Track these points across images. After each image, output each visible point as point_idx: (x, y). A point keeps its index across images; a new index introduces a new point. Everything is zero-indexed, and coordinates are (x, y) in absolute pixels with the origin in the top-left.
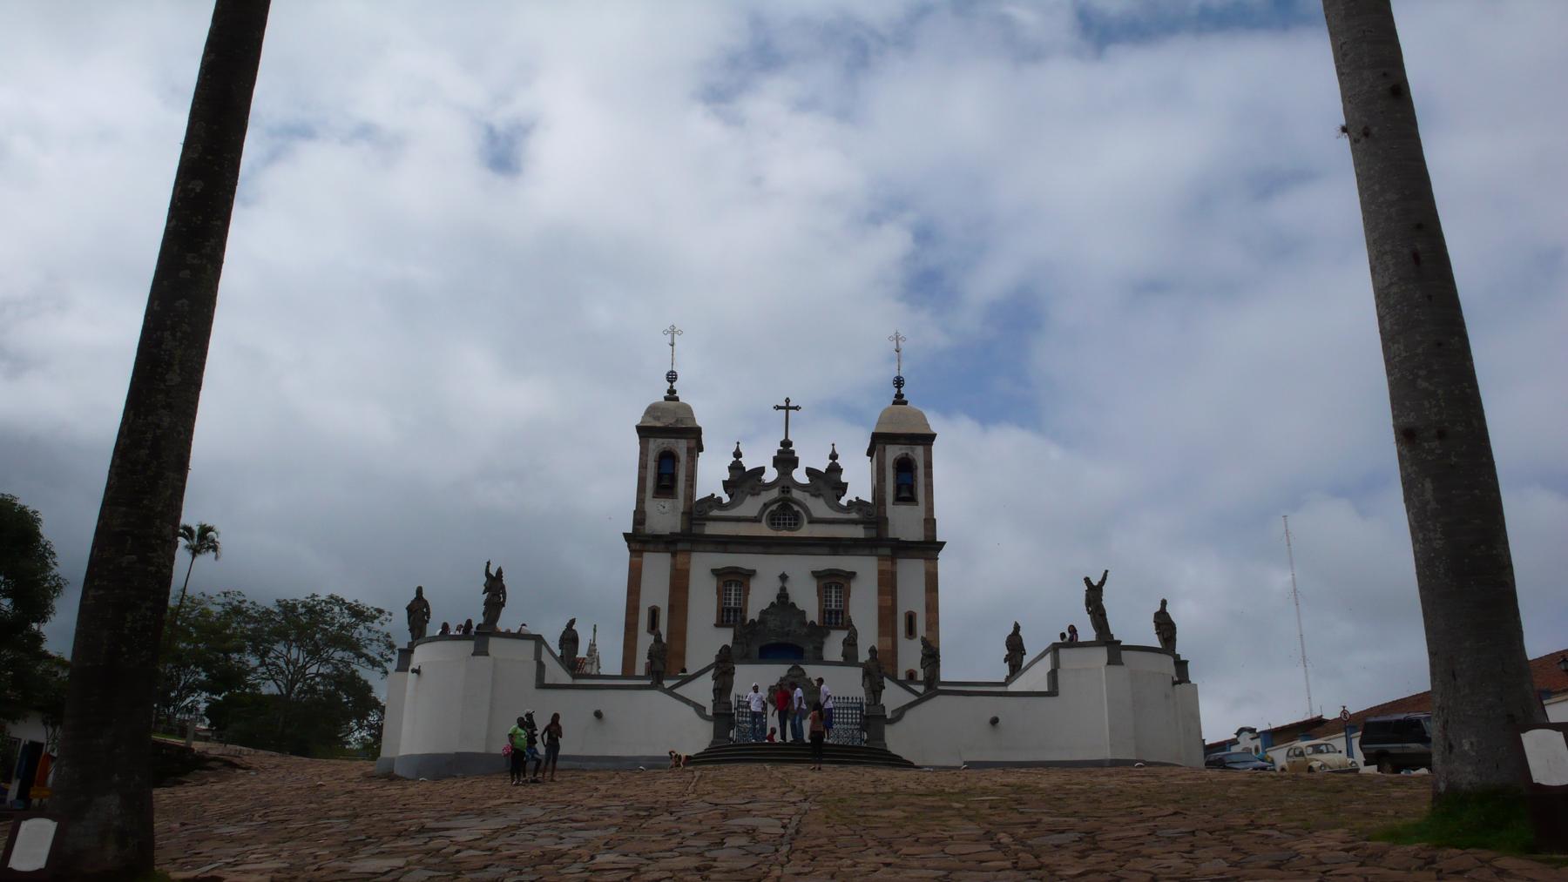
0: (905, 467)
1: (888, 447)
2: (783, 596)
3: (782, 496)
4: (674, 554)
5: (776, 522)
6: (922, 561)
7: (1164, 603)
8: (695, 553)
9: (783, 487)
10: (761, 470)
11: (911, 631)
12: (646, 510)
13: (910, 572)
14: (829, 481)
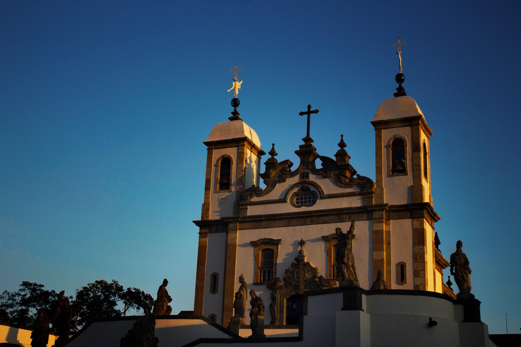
7: (459, 244)
9: (304, 173)
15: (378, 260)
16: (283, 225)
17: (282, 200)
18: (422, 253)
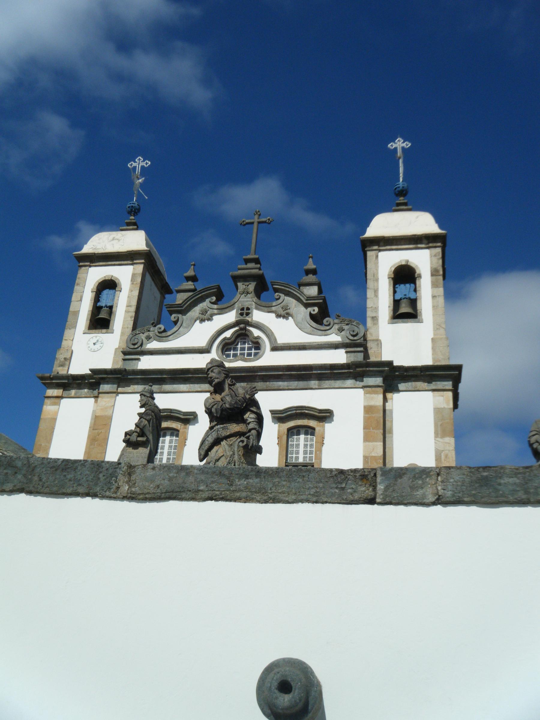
1: (381, 254)
3: (242, 318)
5: (232, 352)
6: (430, 393)
9: (242, 309)
12: (73, 348)
15: (372, 456)
16: (199, 390)
18: (449, 450)
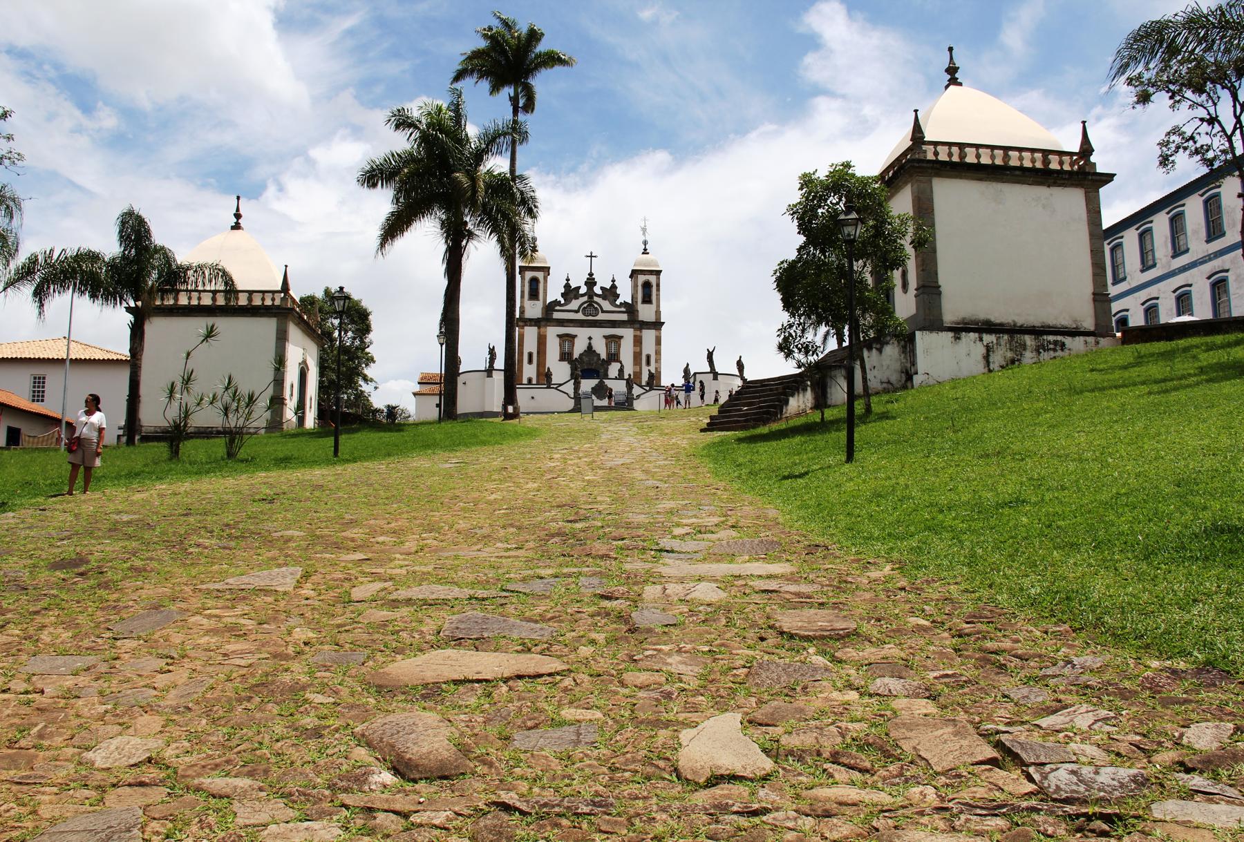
0: (647, 285)
2: (590, 347)
4: (539, 328)
8: (535, 317)
10: (579, 287)
11: (648, 363)
13: (648, 336)
14: (611, 293)
17: (577, 312)
